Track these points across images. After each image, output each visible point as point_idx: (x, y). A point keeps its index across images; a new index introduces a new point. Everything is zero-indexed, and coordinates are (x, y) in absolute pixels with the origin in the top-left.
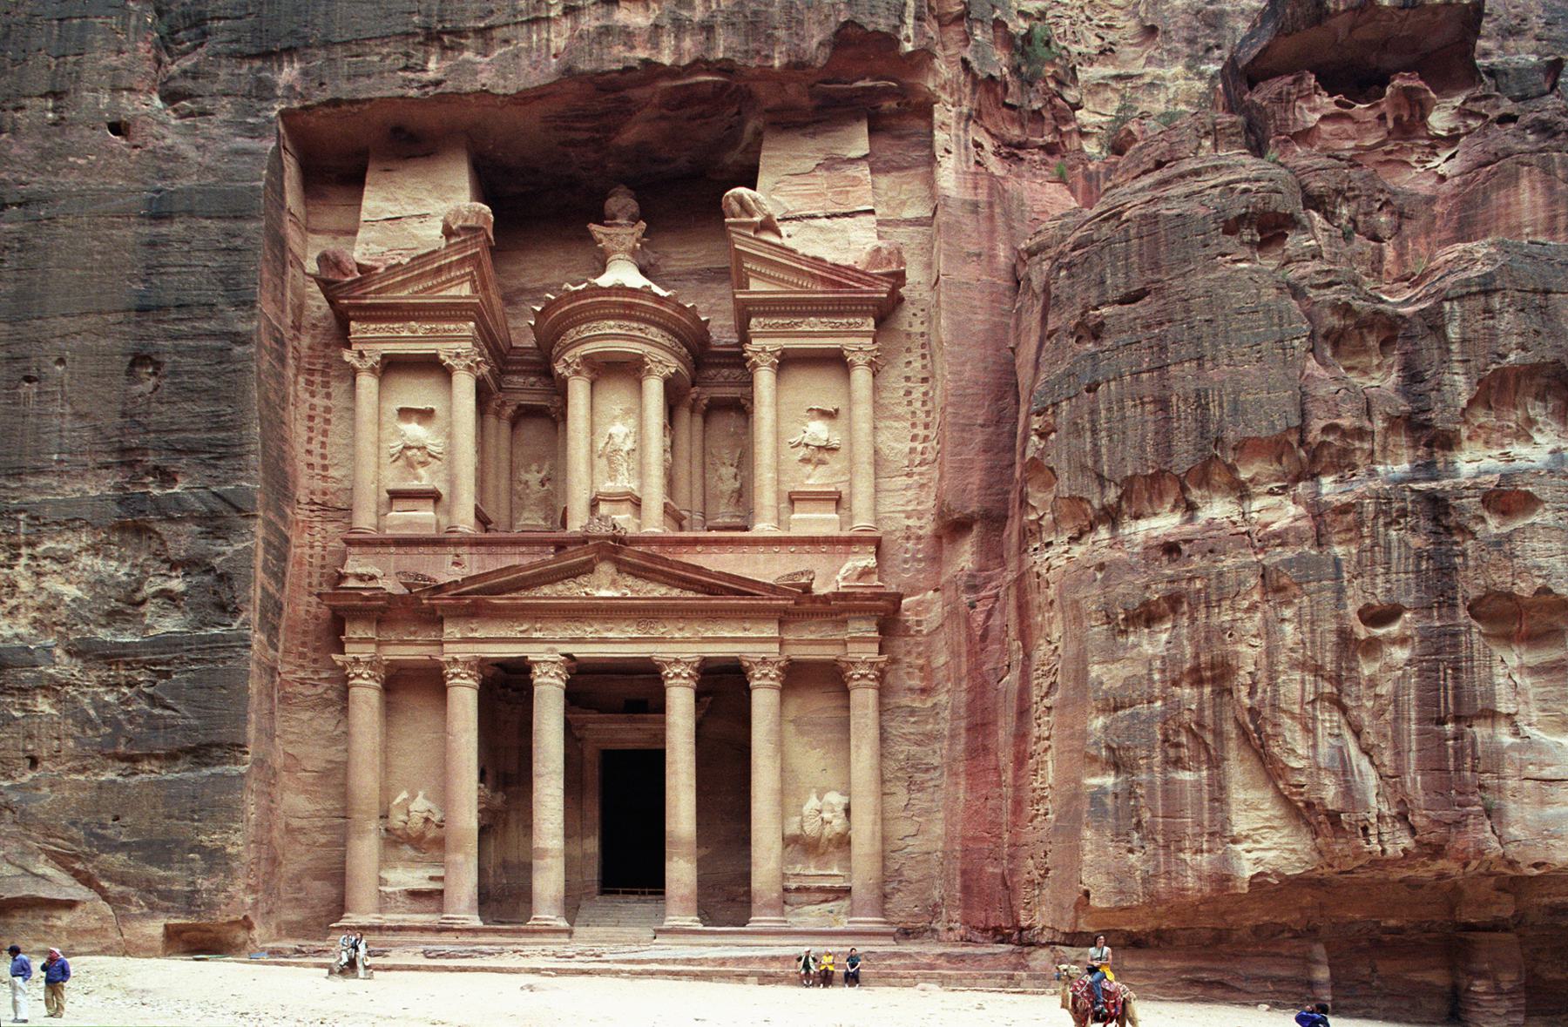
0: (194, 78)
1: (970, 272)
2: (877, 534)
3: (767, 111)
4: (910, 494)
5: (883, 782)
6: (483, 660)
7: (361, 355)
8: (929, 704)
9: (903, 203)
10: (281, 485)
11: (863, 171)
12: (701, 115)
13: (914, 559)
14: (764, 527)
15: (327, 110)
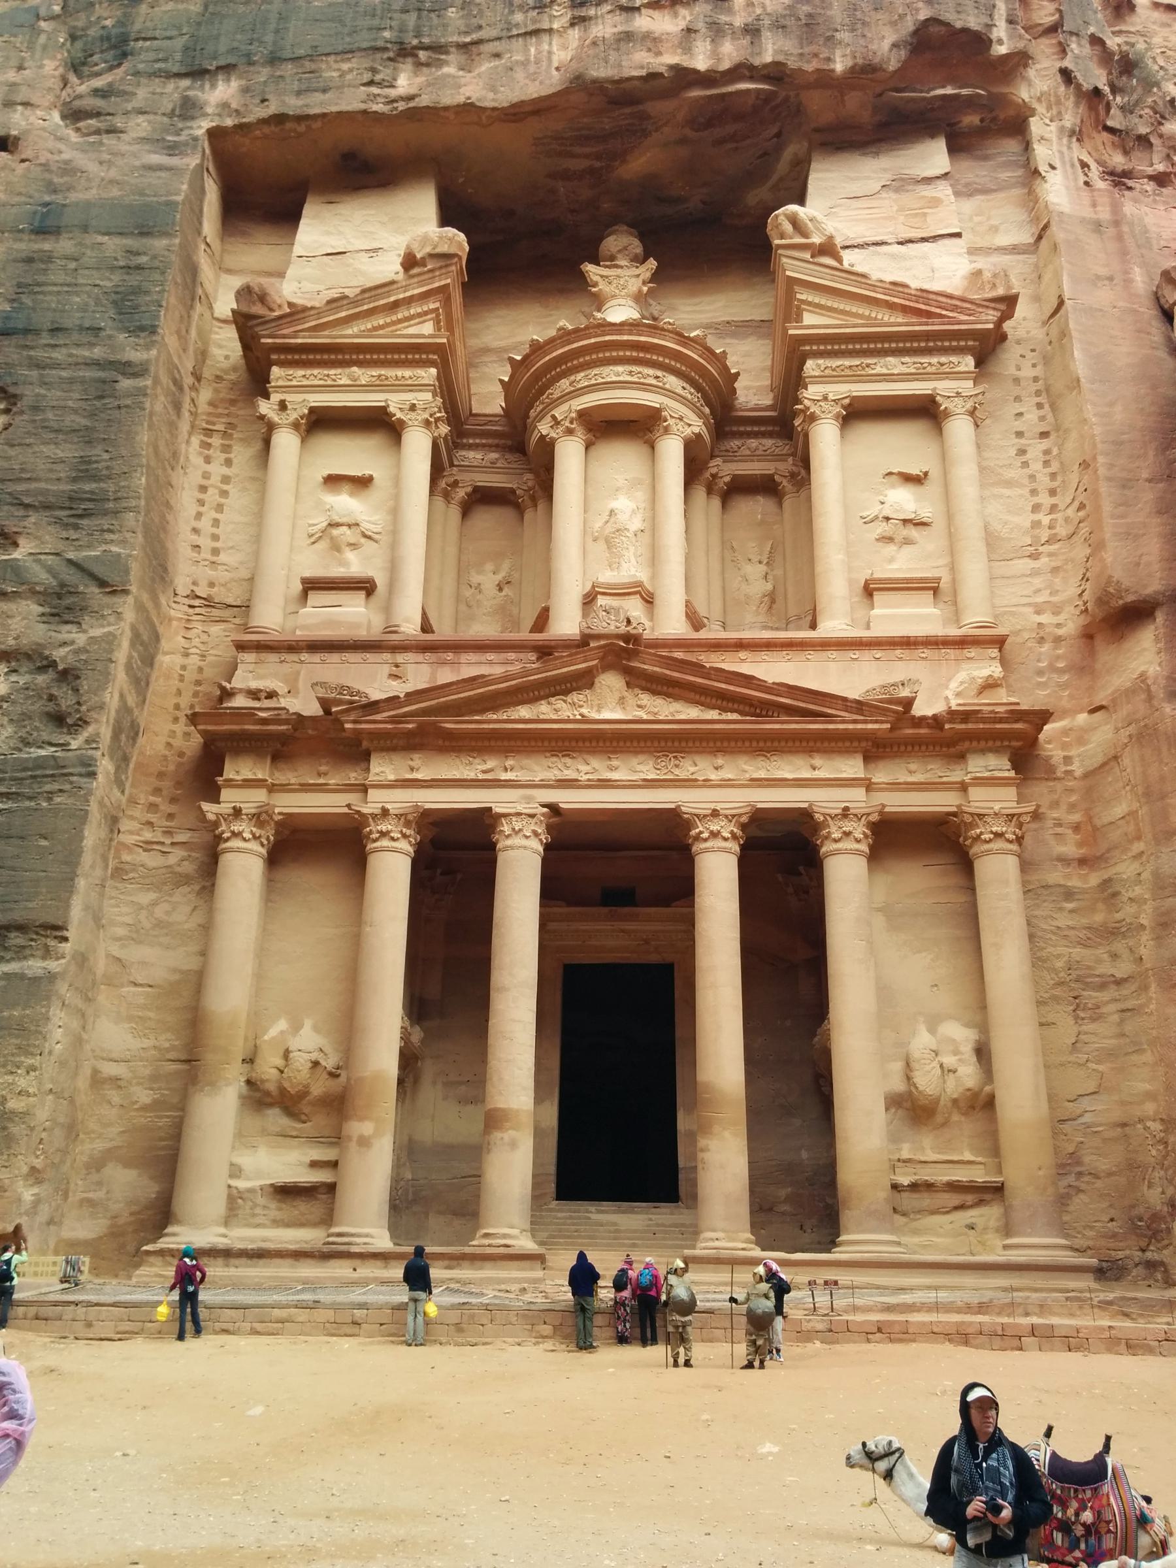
0: (104, 97)
1: (1104, 296)
2: (1000, 631)
3: (817, 130)
4: (1037, 582)
5: (1040, 1003)
6: (426, 813)
7: (283, 406)
8: (1094, 879)
9: (995, 229)
10: (160, 570)
11: (943, 190)
12: (733, 138)
13: (1052, 668)
14: (833, 625)
15: (266, 130)
